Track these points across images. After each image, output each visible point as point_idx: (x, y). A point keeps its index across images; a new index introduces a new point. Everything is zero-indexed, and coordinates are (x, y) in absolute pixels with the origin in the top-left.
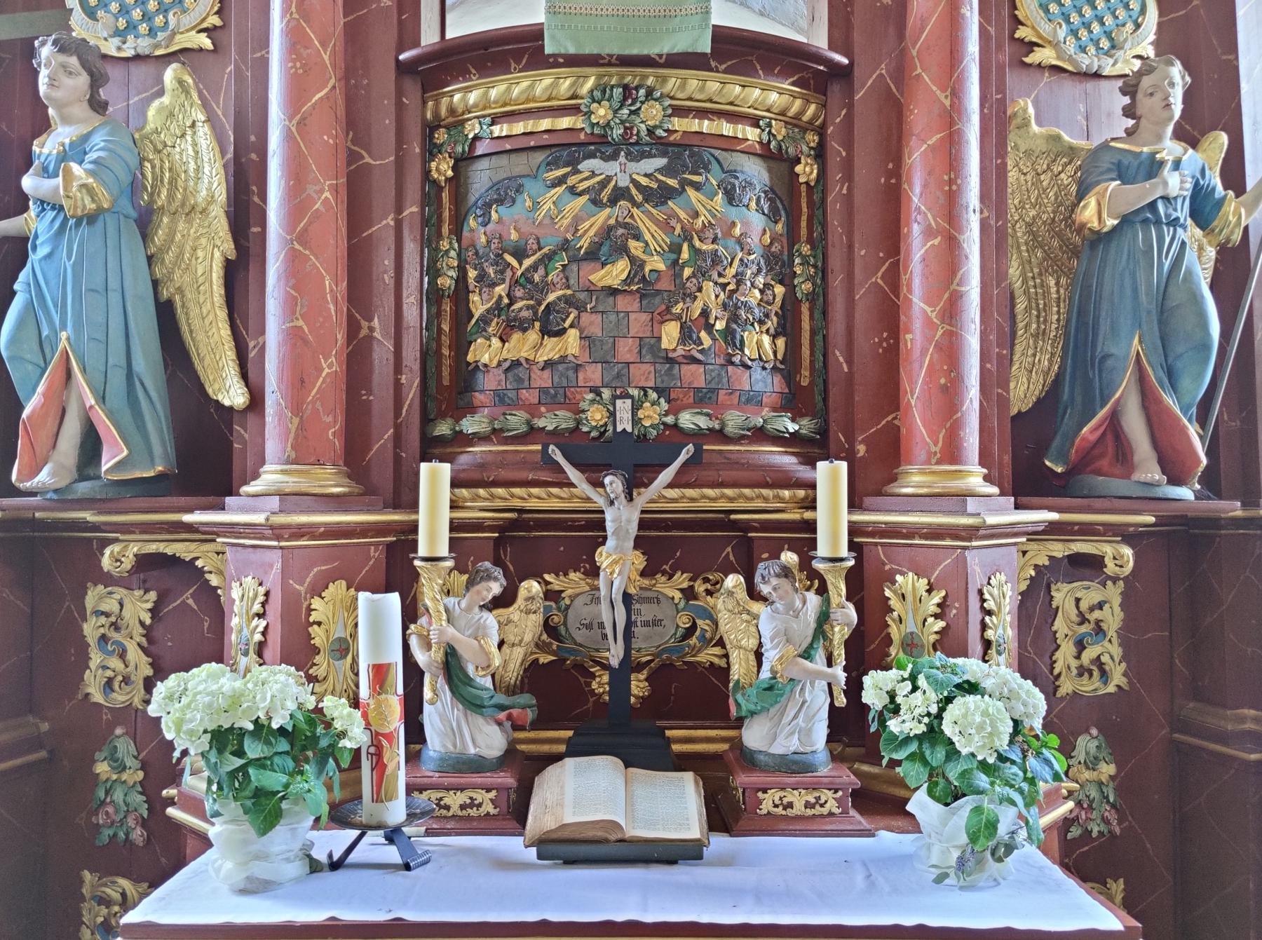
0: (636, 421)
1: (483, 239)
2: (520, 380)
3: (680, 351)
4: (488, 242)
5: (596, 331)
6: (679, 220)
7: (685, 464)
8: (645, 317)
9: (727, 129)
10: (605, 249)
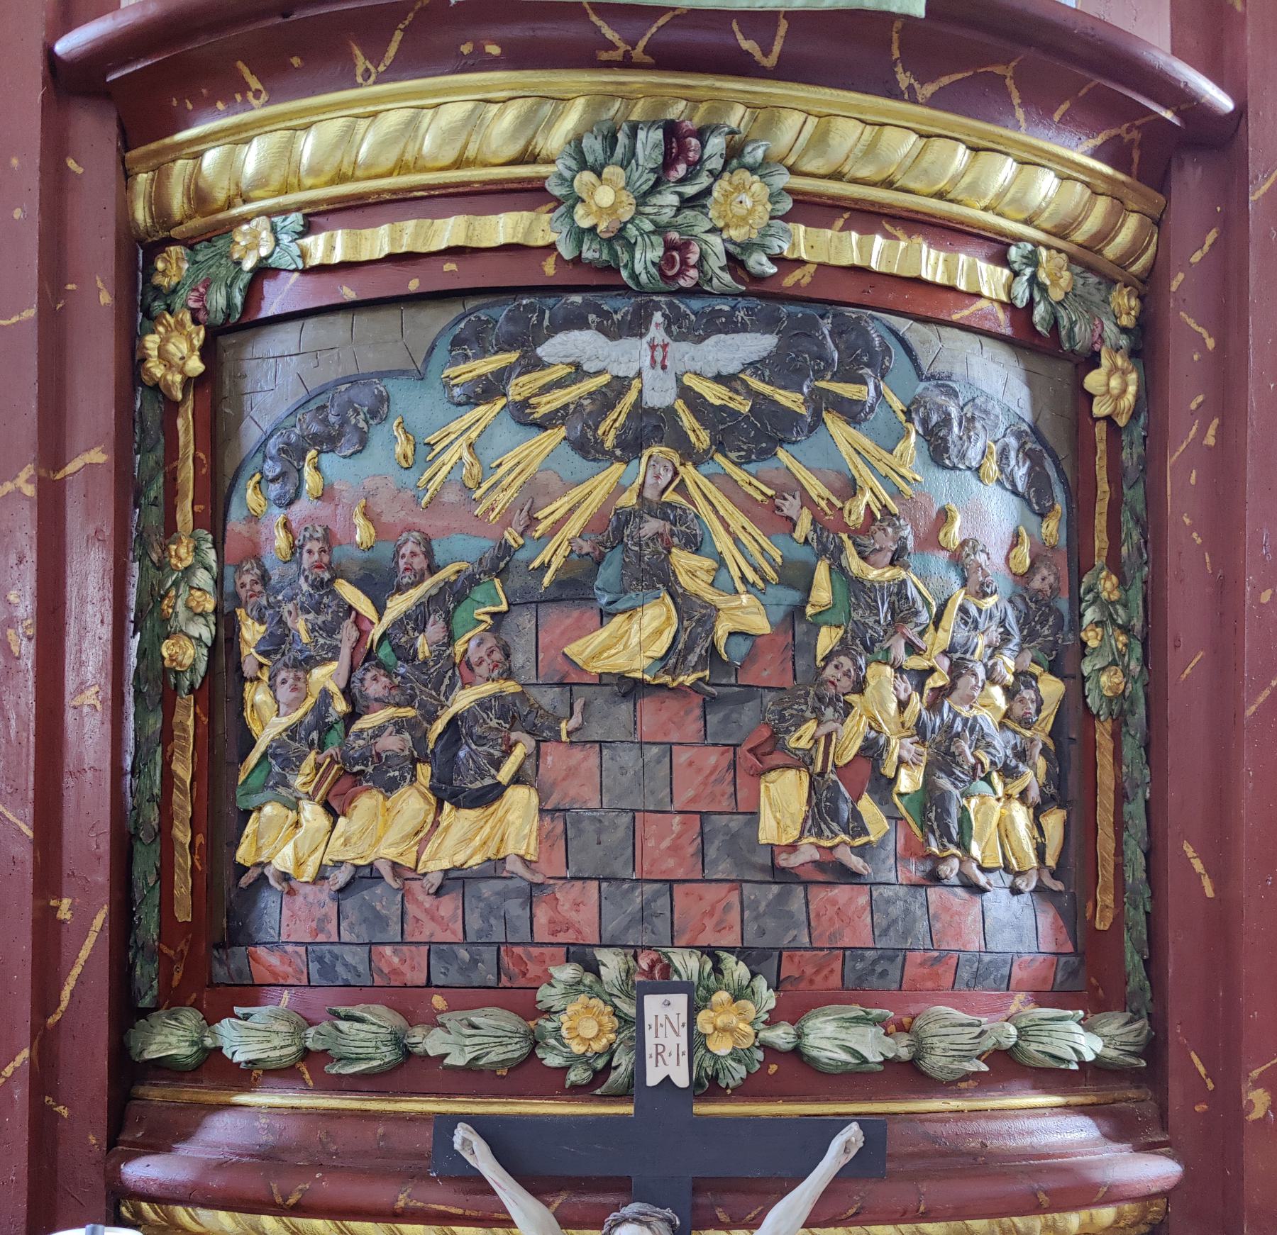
0: (696, 1041)
1: (281, 540)
2: (378, 920)
3: (808, 853)
4: (295, 549)
5: (583, 793)
6: (807, 501)
7: (842, 1177)
8: (713, 758)
10: (608, 574)
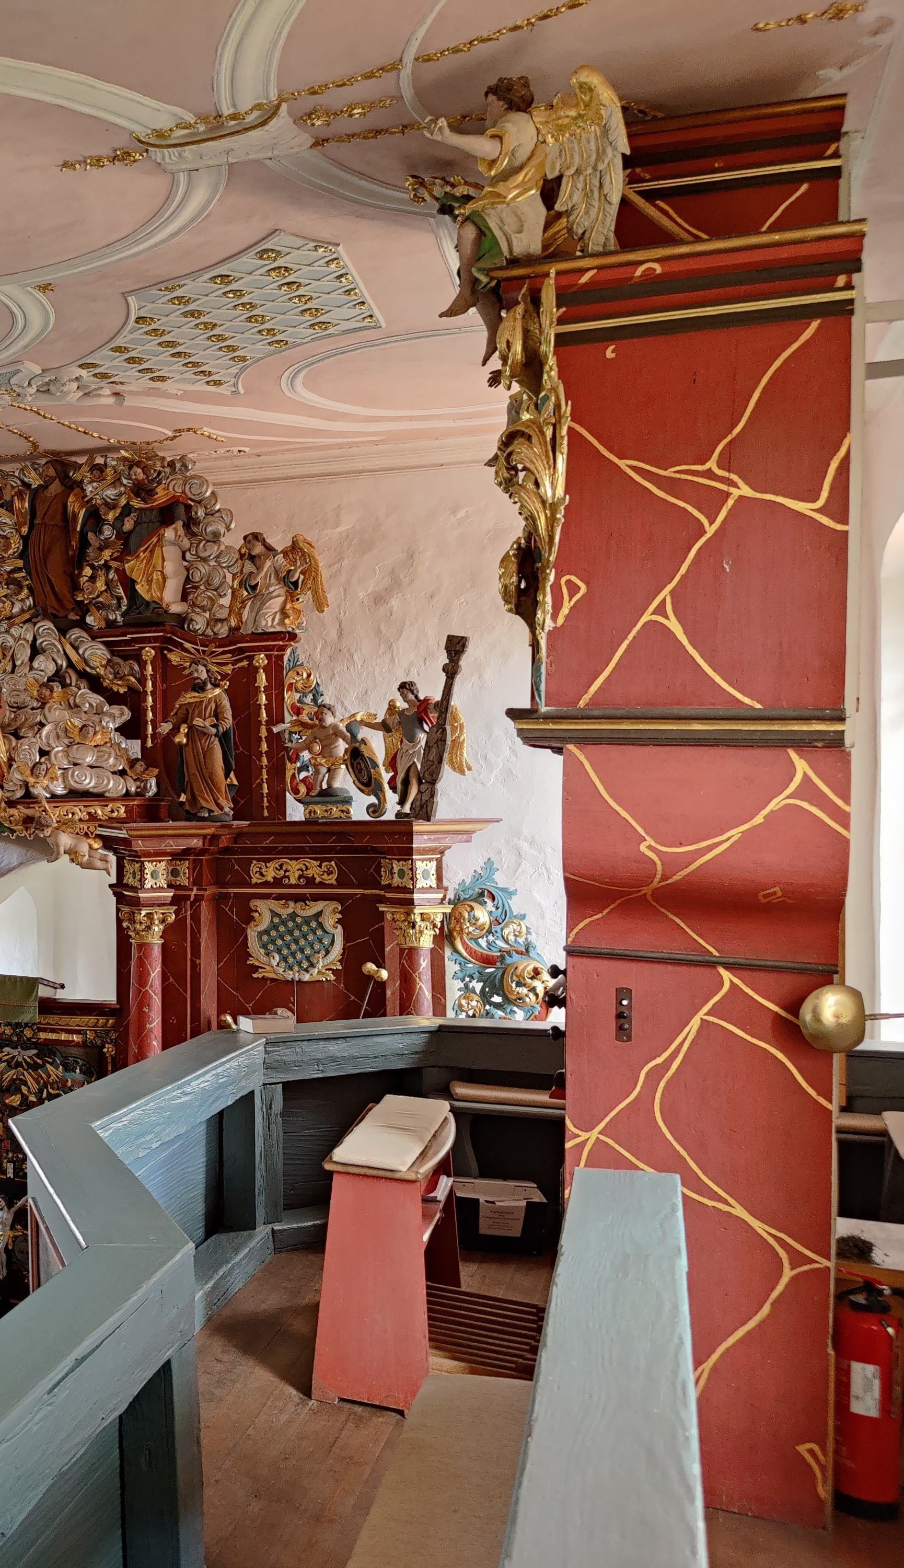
6: (42, 1078)
9: (63, 1037)
